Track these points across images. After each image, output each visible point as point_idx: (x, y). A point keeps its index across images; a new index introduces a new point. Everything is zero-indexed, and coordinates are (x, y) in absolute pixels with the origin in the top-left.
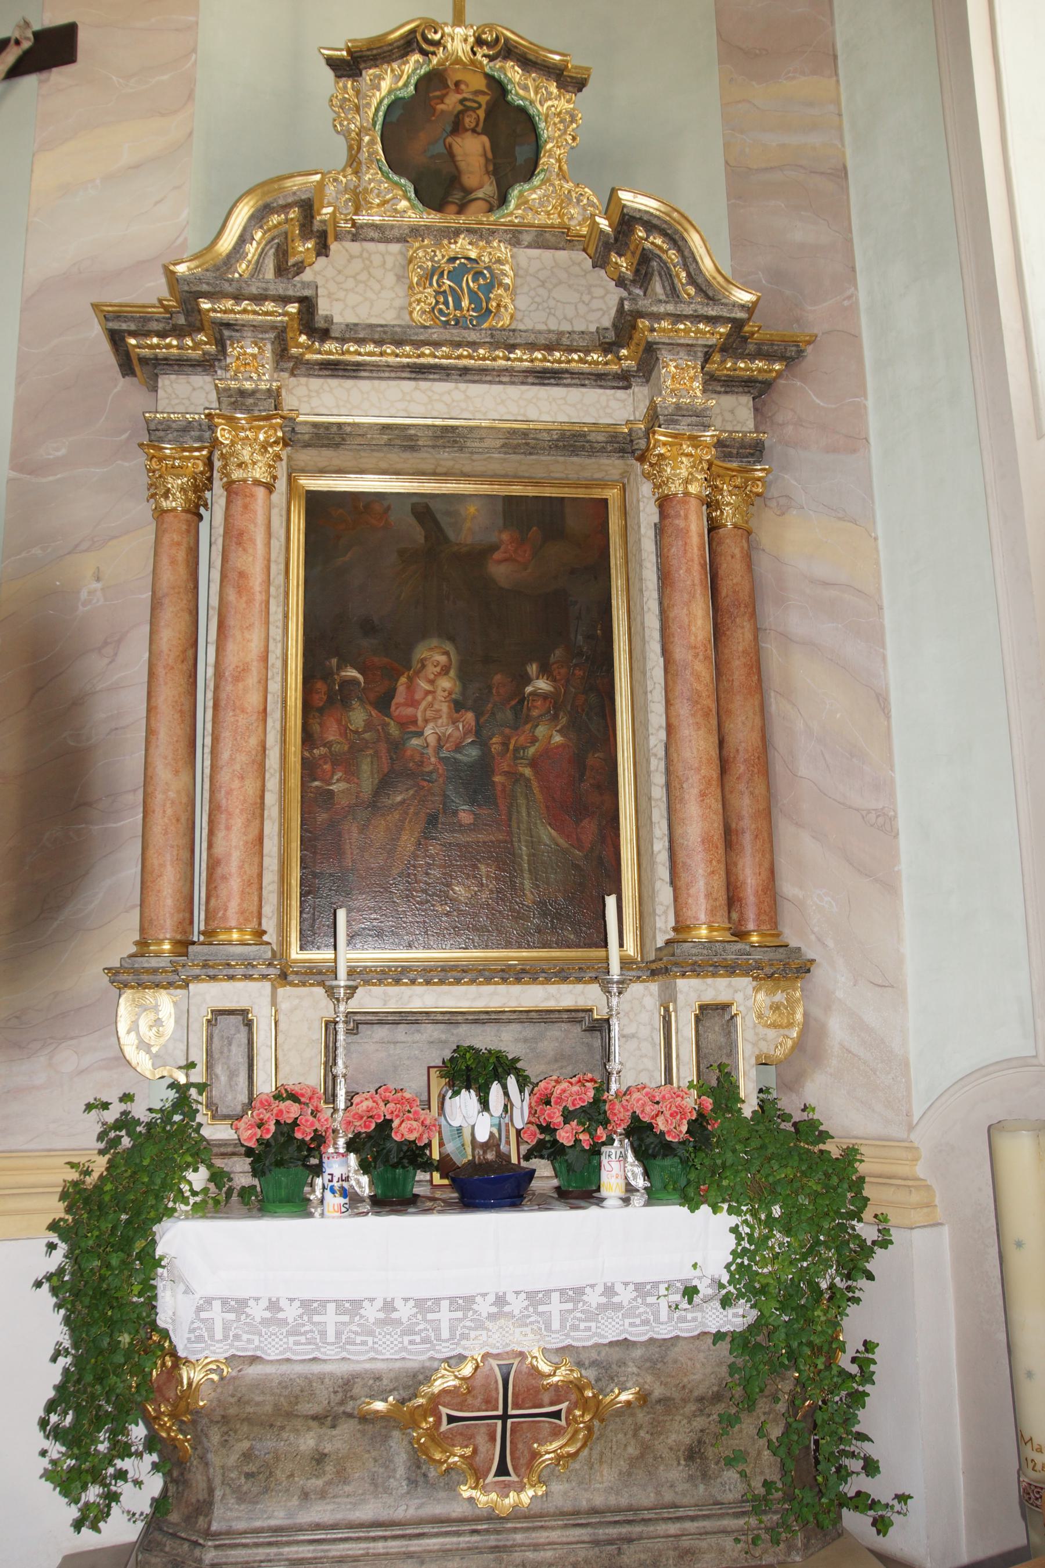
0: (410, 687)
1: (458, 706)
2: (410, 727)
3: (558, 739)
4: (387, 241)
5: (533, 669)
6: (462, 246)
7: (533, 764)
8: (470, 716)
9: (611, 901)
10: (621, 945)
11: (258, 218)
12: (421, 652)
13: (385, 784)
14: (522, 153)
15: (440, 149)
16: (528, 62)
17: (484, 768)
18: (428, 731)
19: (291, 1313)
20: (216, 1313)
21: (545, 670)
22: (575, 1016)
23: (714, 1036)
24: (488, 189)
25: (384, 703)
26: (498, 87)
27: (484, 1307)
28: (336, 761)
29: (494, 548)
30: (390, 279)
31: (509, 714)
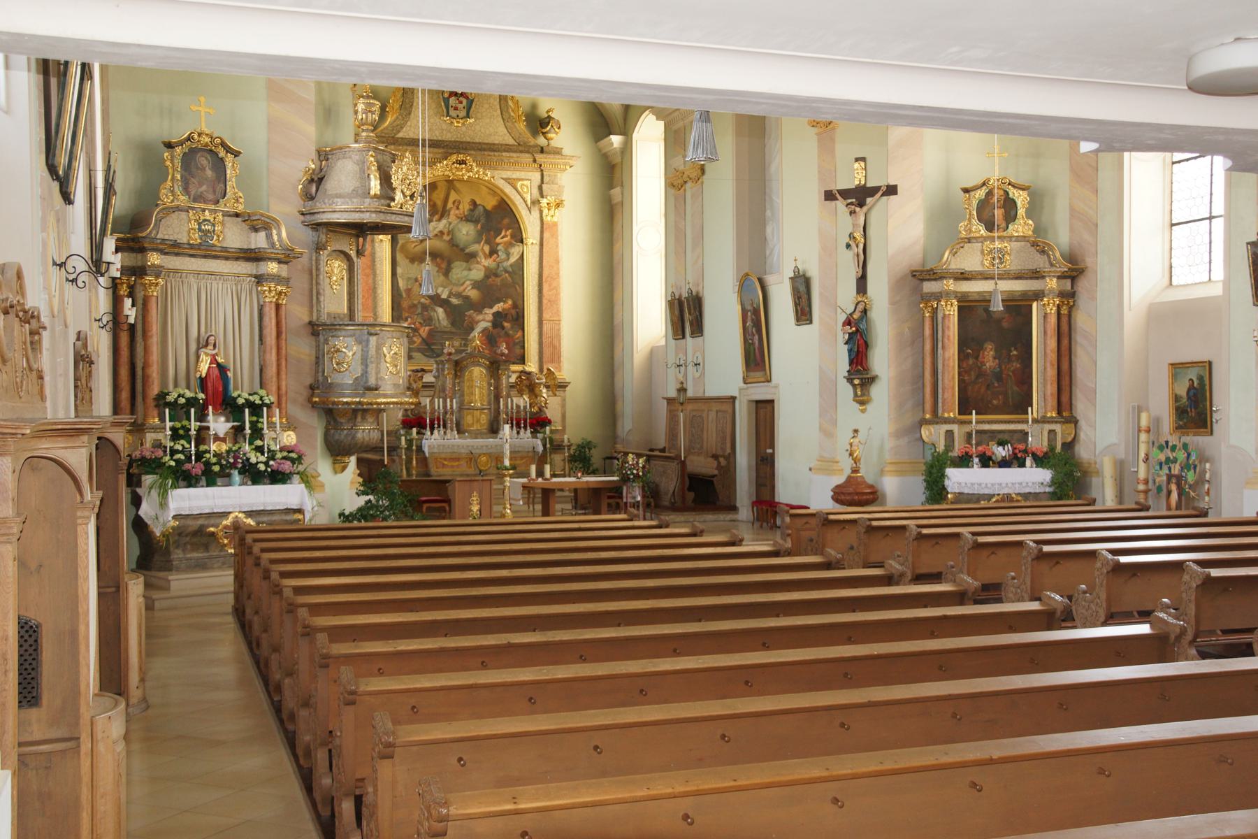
0: (983, 354)
1: (995, 358)
2: (983, 363)
3: (1018, 366)
4: (977, 242)
5: (1013, 349)
6: (997, 244)
7: (1013, 372)
8: (997, 361)
9: (1030, 409)
10: (1032, 413)
11: (950, 253)
12: (986, 345)
13: (977, 377)
14: (1013, 213)
15: (991, 214)
16: (1014, 186)
17: (1001, 372)
18: (988, 364)
19: (969, 485)
20: (956, 485)
21: (1016, 349)
22: (1022, 431)
23: (1052, 436)
24: (1004, 225)
25: (977, 358)
26: (1007, 193)
27: (1004, 485)
28: (966, 372)
29: (1003, 318)
30: (979, 253)
31: (1006, 360)
